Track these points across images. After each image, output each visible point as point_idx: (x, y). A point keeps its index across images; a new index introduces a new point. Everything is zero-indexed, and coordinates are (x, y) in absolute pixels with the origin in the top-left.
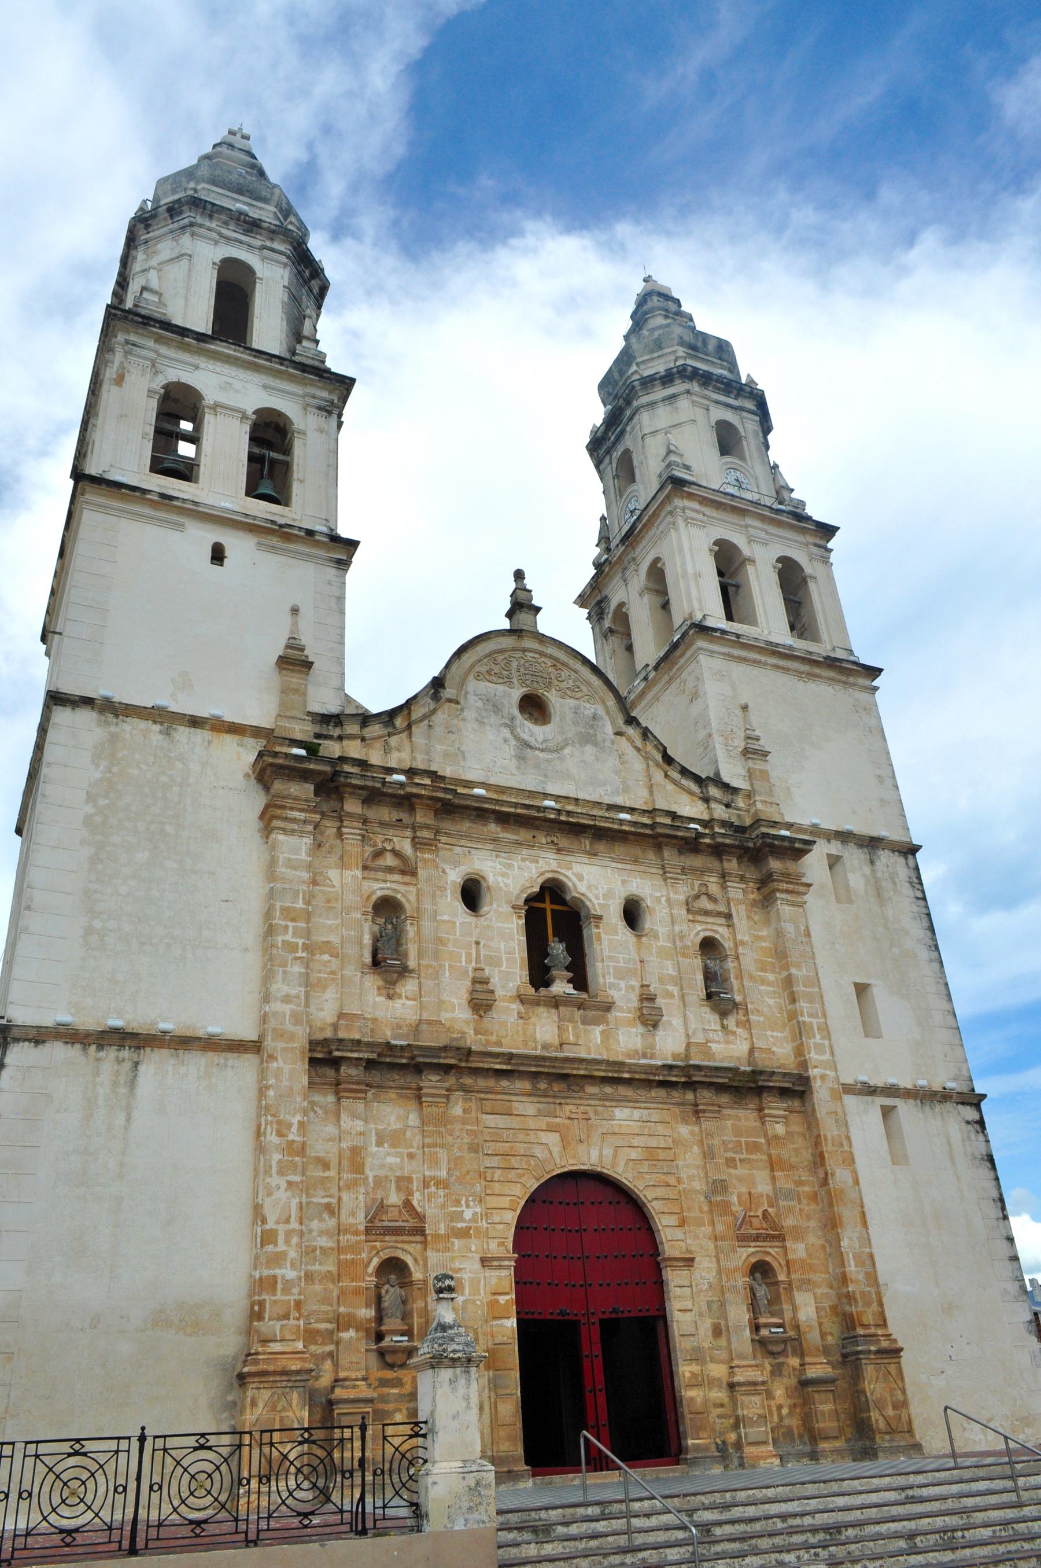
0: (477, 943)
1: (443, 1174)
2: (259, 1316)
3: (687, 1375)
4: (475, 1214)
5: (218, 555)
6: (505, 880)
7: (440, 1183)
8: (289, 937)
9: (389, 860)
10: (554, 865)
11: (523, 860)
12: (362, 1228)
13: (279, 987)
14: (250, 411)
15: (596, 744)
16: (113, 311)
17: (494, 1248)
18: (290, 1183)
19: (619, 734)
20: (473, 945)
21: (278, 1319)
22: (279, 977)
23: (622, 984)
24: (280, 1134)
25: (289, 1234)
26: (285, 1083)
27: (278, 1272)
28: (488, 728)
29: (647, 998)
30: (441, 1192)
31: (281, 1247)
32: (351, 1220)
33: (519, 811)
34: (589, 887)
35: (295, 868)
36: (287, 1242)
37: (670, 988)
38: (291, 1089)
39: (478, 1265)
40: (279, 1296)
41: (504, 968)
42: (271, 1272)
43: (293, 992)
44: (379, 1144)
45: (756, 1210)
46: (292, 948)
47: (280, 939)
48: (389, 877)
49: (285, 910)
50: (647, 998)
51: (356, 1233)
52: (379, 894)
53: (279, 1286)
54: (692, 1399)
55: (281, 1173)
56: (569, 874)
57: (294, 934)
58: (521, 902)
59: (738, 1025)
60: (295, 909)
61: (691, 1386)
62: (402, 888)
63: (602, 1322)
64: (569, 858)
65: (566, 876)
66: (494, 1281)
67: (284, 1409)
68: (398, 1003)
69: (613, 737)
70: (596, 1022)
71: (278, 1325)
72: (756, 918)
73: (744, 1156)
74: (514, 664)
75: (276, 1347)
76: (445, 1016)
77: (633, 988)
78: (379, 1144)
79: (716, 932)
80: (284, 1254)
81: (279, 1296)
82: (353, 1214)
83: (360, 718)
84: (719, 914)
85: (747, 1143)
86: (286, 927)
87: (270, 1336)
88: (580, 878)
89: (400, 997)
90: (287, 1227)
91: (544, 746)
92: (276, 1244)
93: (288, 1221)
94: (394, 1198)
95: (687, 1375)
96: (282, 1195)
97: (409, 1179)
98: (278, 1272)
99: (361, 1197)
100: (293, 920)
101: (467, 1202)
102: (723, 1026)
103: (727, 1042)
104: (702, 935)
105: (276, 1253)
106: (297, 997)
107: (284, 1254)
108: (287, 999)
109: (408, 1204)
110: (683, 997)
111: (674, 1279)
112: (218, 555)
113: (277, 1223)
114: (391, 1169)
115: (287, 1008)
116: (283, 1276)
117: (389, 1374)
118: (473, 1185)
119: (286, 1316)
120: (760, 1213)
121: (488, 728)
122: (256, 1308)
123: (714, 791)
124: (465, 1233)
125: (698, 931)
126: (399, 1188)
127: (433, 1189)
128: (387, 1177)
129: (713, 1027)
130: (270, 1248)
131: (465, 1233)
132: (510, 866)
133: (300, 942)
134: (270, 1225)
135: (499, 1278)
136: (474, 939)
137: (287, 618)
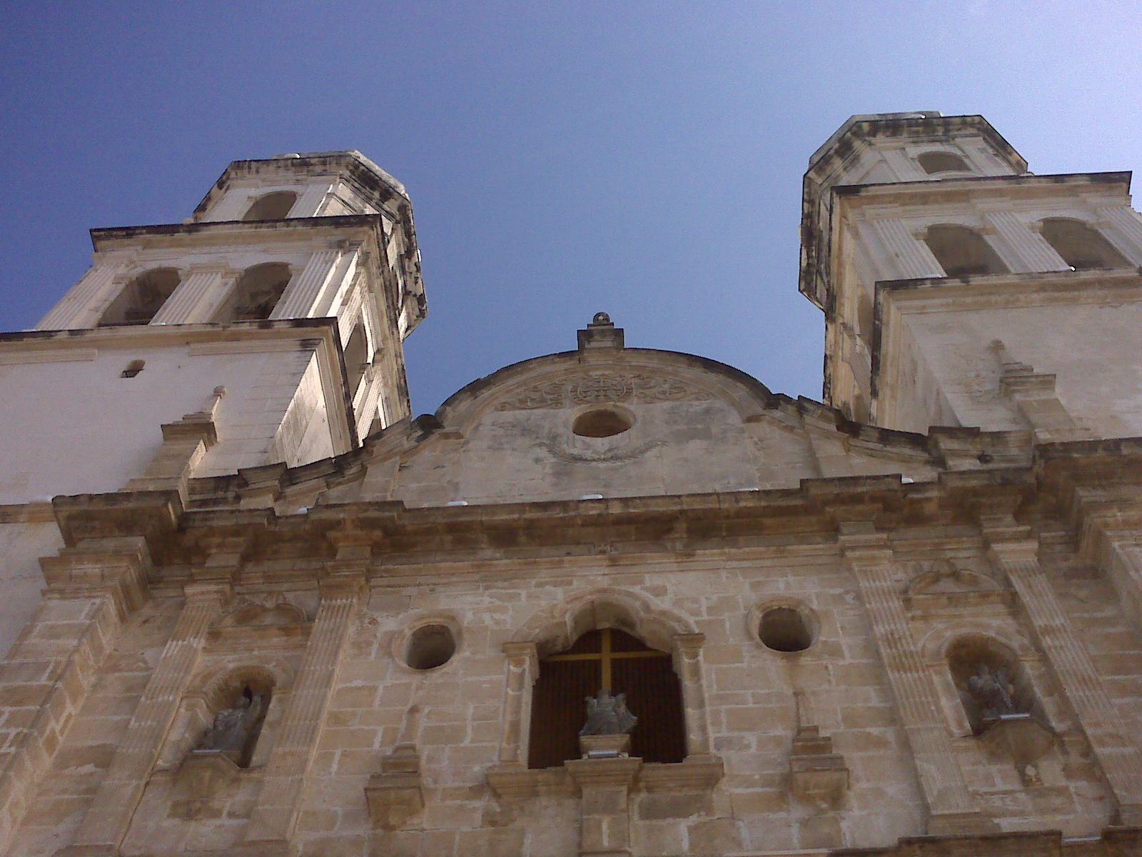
6: (497, 616)
10: (604, 582)
11: (540, 585)
16: (95, 233)
23: (751, 738)
33: (528, 515)
37: (875, 731)
41: (467, 742)
52: (231, 666)
56: (637, 589)
59: (1068, 772)
64: (636, 569)
65: (629, 594)
70: (678, 810)
72: (1083, 593)
77: (778, 741)
83: (280, 471)
88: (660, 592)
89: (216, 814)
91: (609, 455)
102: (1026, 781)
110: (905, 744)
123: (946, 444)
129: (1001, 786)
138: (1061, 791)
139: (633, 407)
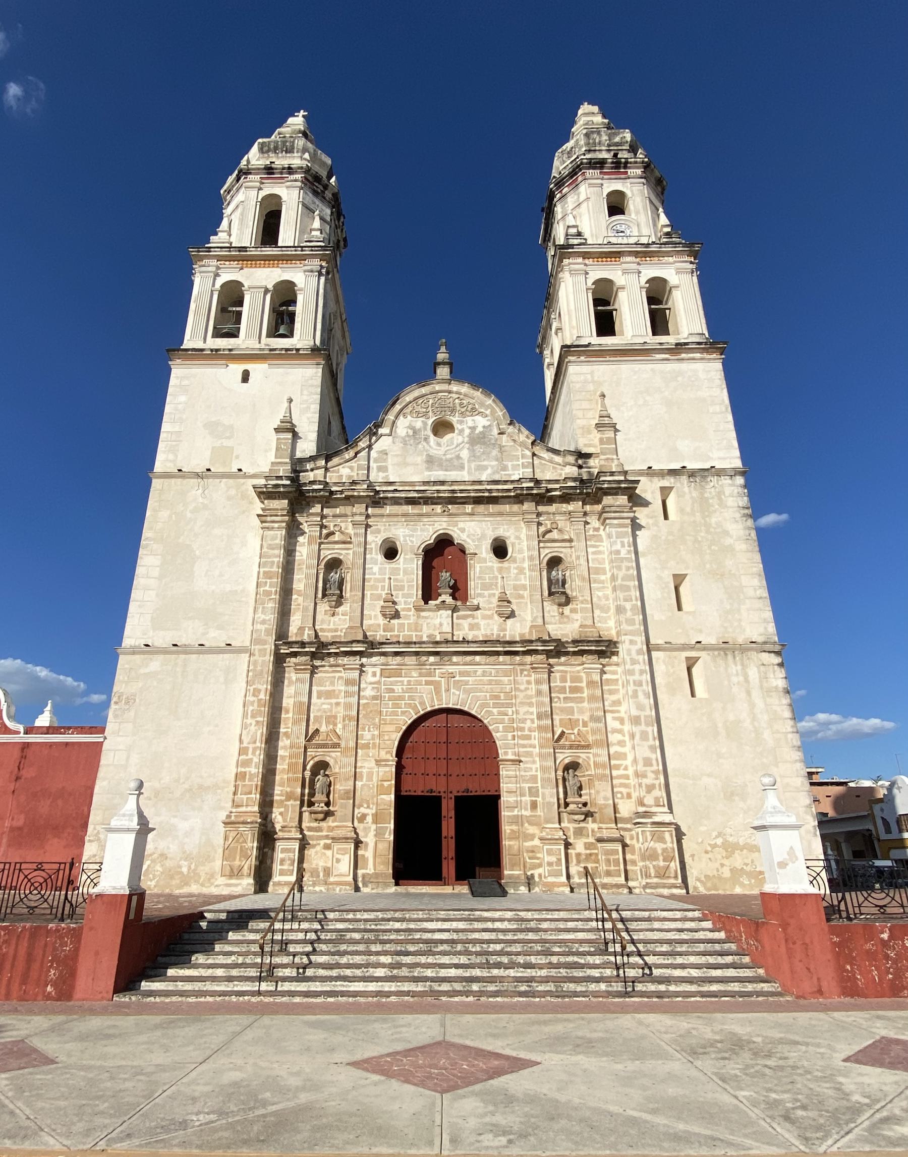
0: (390, 579)
3: (508, 831)
4: (373, 735)
5: (246, 377)
8: (267, 588)
9: (337, 537)
10: (445, 525)
13: (260, 616)
14: (270, 287)
15: (484, 443)
17: (383, 755)
18: (257, 722)
20: (387, 581)
21: (245, 794)
22: (260, 610)
23: (486, 593)
24: (254, 695)
25: (254, 749)
26: (259, 668)
28: (409, 447)
29: (504, 600)
31: (250, 756)
34: (468, 536)
35: (273, 549)
36: (254, 753)
37: (521, 592)
38: (262, 671)
39: (373, 764)
40: (247, 782)
41: (406, 591)
42: (243, 770)
43: (267, 618)
45: (573, 730)
46: (268, 593)
47: (262, 589)
48: (337, 546)
49: (265, 572)
50: (504, 600)
51: (299, 748)
54: (510, 846)
55: (253, 716)
56: (455, 529)
57: (270, 586)
60: (271, 572)
61: (510, 839)
62: (343, 552)
63: (455, 797)
66: (381, 774)
68: (336, 618)
69: (497, 436)
71: (245, 797)
73: (568, 695)
74: (431, 401)
75: (243, 809)
77: (494, 595)
78: (319, 697)
79: (561, 552)
80: (251, 759)
81: (247, 782)
82: (298, 738)
84: (564, 541)
85: (570, 687)
86: (266, 582)
90: (254, 745)
92: (247, 755)
93: (255, 742)
95: (508, 831)
96: (253, 728)
97: (335, 717)
98: (247, 769)
100: (270, 578)
101: (369, 728)
103: (561, 623)
104: (550, 556)
105: (247, 760)
106: (270, 620)
107: (251, 759)
108: (263, 622)
111: (505, 772)
112: (246, 377)
113: (249, 743)
114: (325, 712)
115: (263, 627)
117: (315, 824)
118: (374, 719)
119: (250, 793)
120: (576, 731)
121: (409, 447)
124: (366, 746)
125: (547, 553)
126: (328, 723)
127: (347, 722)
128: (322, 716)
130: (242, 757)
132: (415, 530)
133: (274, 590)
134: (245, 745)
135: (385, 772)
136: (387, 577)
137: (286, 405)
138: (567, 617)
139: (454, 420)
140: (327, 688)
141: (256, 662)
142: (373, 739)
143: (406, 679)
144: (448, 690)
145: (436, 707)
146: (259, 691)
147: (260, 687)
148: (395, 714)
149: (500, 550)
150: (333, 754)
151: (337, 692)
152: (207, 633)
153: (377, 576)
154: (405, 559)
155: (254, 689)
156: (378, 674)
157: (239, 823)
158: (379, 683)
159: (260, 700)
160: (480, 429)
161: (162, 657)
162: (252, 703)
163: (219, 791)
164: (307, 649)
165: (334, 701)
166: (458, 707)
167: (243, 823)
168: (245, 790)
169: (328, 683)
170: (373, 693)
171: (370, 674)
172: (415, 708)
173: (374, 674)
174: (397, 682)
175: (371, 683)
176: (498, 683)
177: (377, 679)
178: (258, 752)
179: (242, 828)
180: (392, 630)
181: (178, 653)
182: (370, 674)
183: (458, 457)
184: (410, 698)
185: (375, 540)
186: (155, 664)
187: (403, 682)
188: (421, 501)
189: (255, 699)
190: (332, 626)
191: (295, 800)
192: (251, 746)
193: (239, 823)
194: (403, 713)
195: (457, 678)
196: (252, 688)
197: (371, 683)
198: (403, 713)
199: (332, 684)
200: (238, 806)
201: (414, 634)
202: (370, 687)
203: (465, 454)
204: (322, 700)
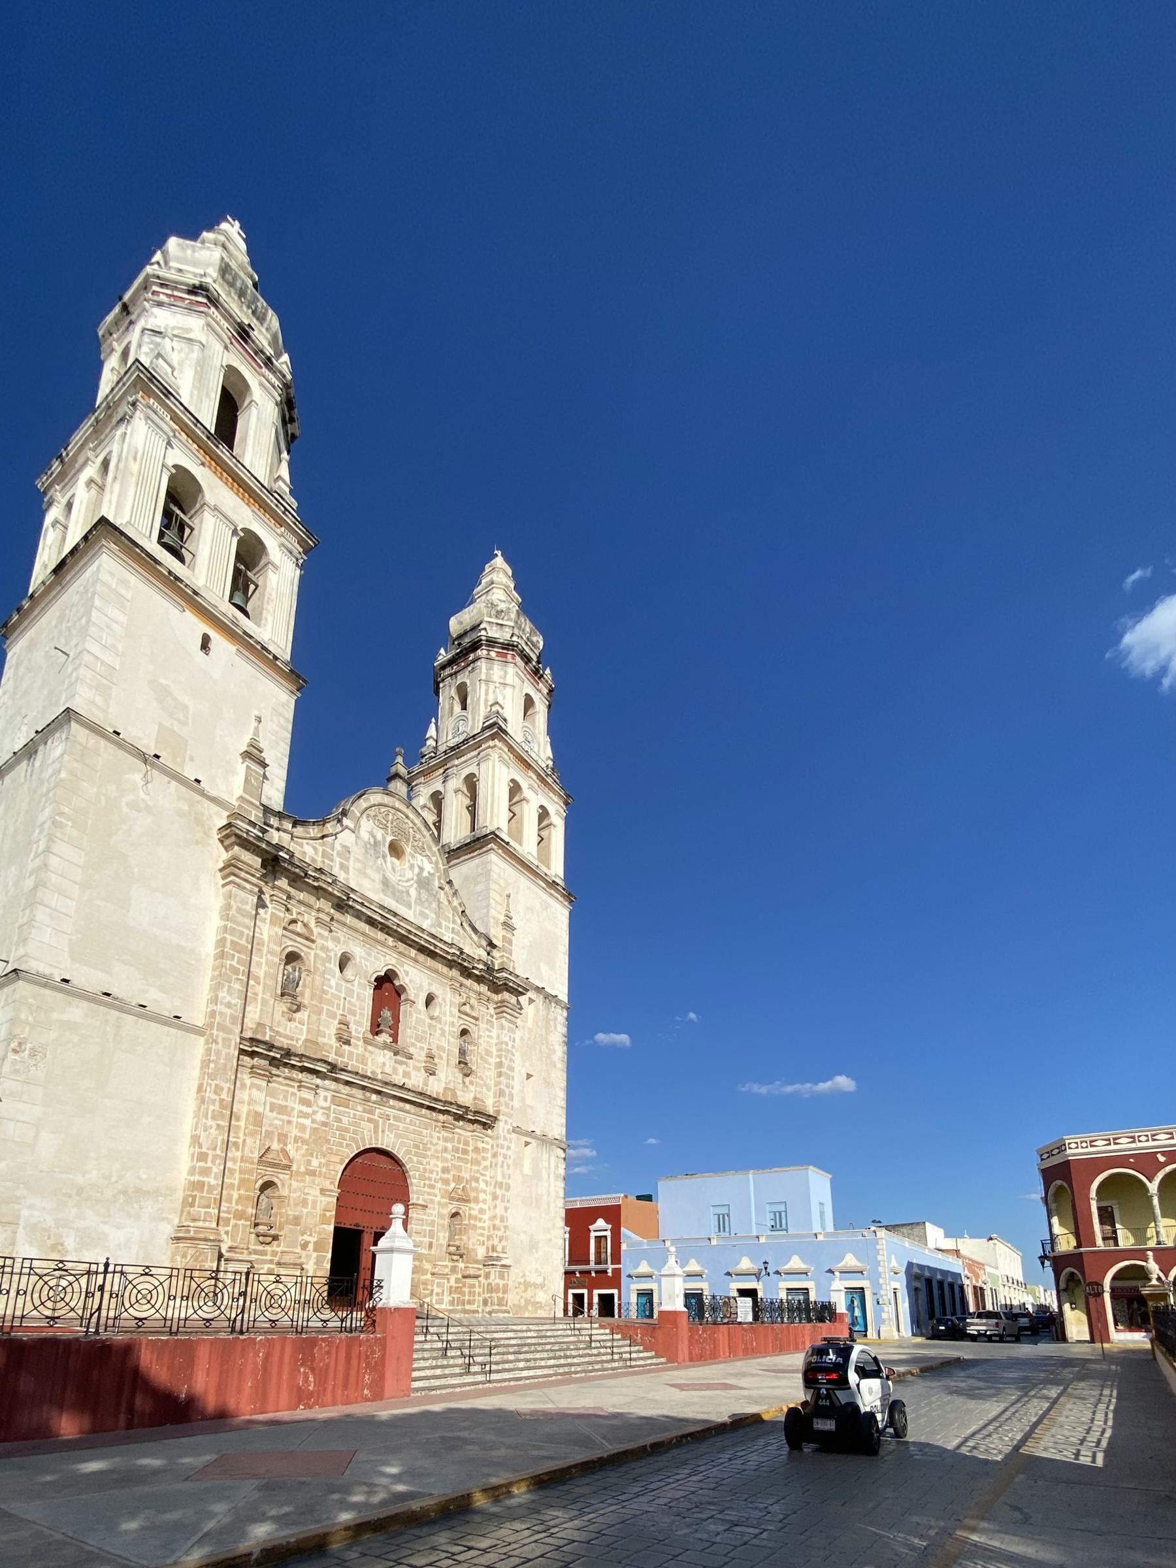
0: (345, 999)
1: (307, 1136)
2: (192, 1205)
4: (320, 1163)
7: (304, 1142)
12: (256, 1161)
18: (218, 1126)
19: (441, 888)
20: (342, 1000)
24: (215, 1092)
25: (215, 1157)
27: (205, 1179)
30: (305, 1147)
31: (209, 1164)
32: (250, 1155)
36: (213, 1162)
40: (205, 1194)
42: (201, 1179)
44: (272, 1111)
51: (252, 1163)
53: (206, 1188)
55: (214, 1118)
58: (373, 979)
67: (202, 1261)
68: (293, 1025)
71: (203, 1210)
76: (321, 1040)
78: (272, 1111)
80: (210, 1168)
81: (205, 1194)
87: (197, 1218)
90: (214, 1153)
93: (215, 1149)
94: (275, 1146)
96: (213, 1131)
97: (286, 1136)
98: (205, 1179)
99: (258, 1142)
107: (210, 1168)
109: (284, 1151)
113: (208, 1149)
114: (276, 1128)
116: (209, 1183)
118: (322, 1146)
119: (208, 1207)
122: (190, 1199)
124: (312, 1173)
126: (279, 1141)
127: (300, 1144)
128: (273, 1132)
131: (312, 1173)
134: (204, 1150)
140: (280, 1102)
141: (218, 1053)
142: (320, 1167)
143: (352, 1112)
144: (383, 1131)
145: (374, 1146)
146: (222, 1089)
147: (223, 1084)
148: (340, 1145)
149: (429, 1000)
150: (281, 1176)
151: (289, 1109)
152: (147, 992)
153: (334, 991)
154: (359, 982)
155: (216, 1085)
156: (329, 1099)
157: (200, 1239)
158: (329, 1109)
159: (222, 1101)
160: (425, 874)
161: (85, 1004)
162: (214, 1102)
163: (160, 1199)
164: (272, 1054)
165: (285, 1118)
166: (389, 1149)
167: (206, 1240)
168: (205, 1203)
169: (281, 1097)
170: (323, 1119)
171: (322, 1098)
172: (356, 1142)
173: (325, 1099)
174: (345, 1112)
175: (322, 1108)
176: (420, 1134)
177: (327, 1105)
178: (217, 1162)
179: (202, 1245)
180: (342, 1056)
181: (110, 1006)
182: (322, 1098)
183: (408, 893)
184: (355, 1132)
185: (337, 951)
186: (77, 1011)
187: (349, 1113)
188: (380, 926)
189: (217, 1097)
190: (288, 1032)
191: (246, 1220)
192: (211, 1153)
193: (200, 1239)
194: (348, 1145)
195: (391, 1121)
196: (213, 1083)
197: (322, 1108)
198: (348, 1145)
199: (285, 1098)
200: (194, 1220)
201: (361, 1066)
202: (321, 1111)
203: (413, 892)
204: (275, 1114)
